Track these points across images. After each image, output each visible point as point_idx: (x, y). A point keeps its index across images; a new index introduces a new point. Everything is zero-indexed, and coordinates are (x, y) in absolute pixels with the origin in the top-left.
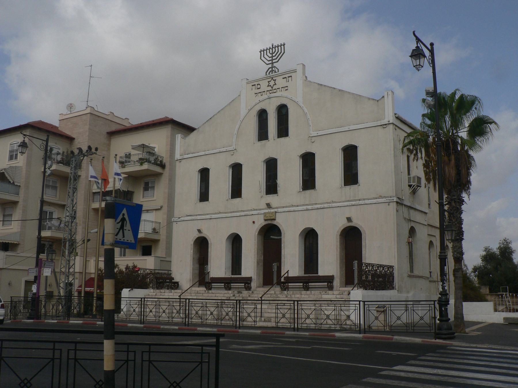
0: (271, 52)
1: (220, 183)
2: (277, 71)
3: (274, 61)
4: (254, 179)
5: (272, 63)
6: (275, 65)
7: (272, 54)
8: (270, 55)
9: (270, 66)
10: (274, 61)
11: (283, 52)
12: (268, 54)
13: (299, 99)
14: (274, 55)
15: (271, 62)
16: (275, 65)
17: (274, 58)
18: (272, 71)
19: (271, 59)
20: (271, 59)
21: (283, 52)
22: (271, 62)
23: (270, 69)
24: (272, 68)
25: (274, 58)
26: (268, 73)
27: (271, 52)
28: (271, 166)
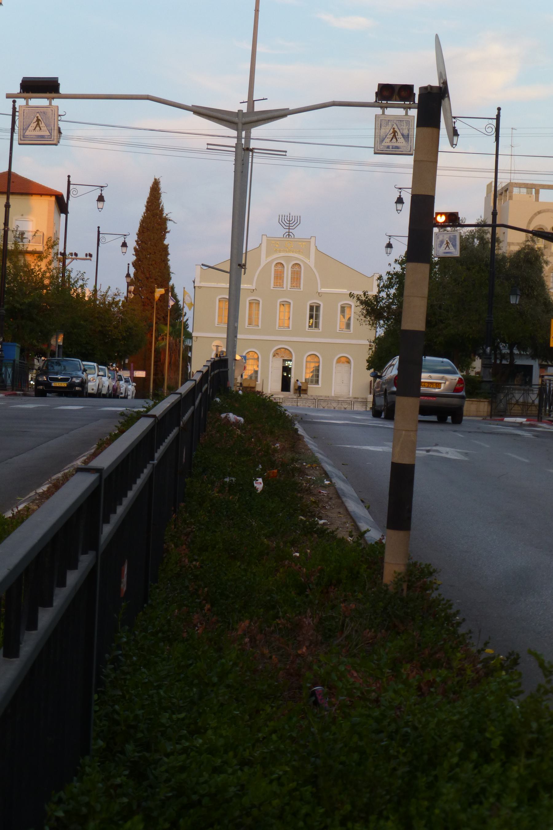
2: (293, 236)
3: (290, 228)
6: (291, 231)
9: (287, 230)
14: (291, 222)
16: (291, 231)
24: (289, 232)
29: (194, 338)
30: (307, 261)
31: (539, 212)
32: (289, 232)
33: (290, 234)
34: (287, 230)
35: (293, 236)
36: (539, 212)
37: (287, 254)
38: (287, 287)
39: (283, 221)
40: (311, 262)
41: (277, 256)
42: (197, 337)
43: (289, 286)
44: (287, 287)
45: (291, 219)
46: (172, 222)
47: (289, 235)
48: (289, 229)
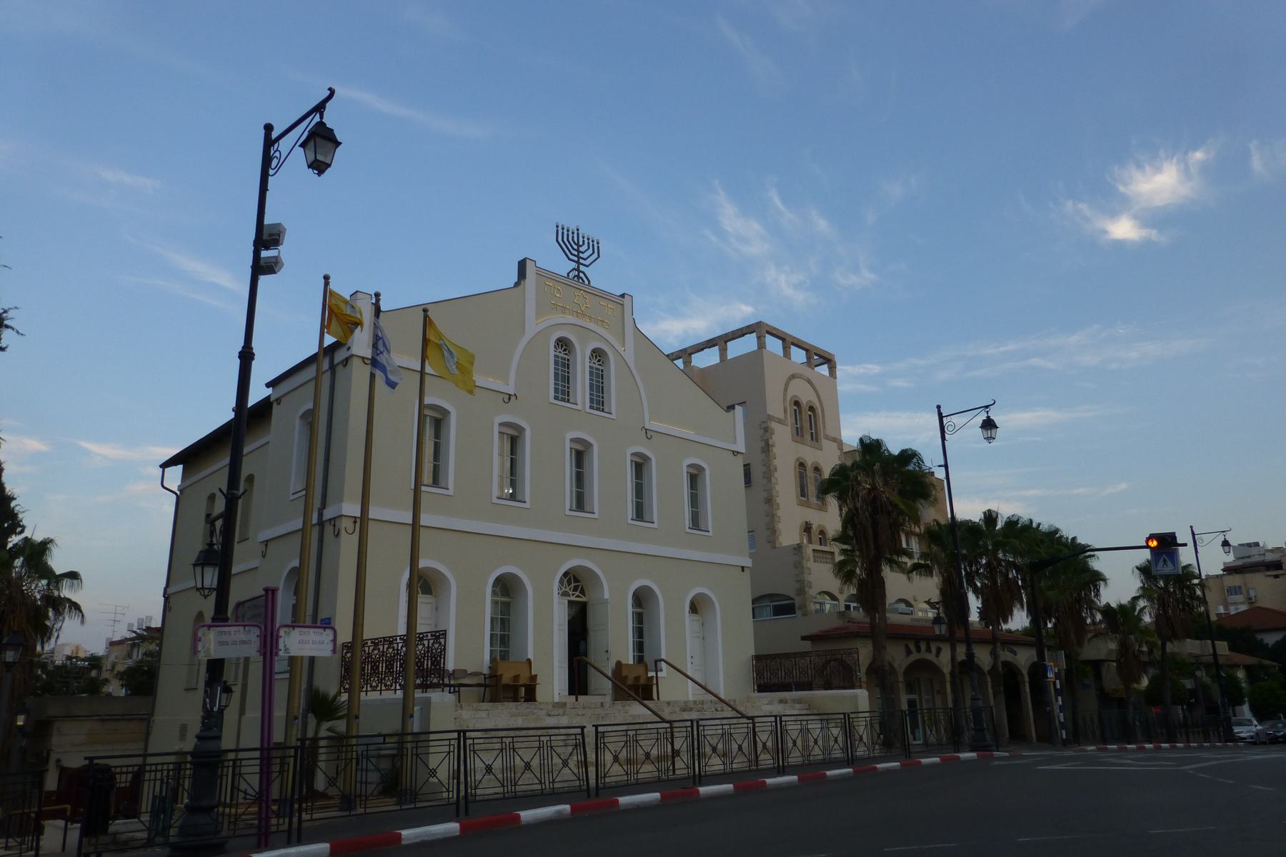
6: (582, 268)
7: (578, 244)
9: (574, 265)
13: (629, 355)
14: (582, 249)
18: (578, 276)
26: (571, 275)
30: (621, 349)
31: (793, 377)
32: (579, 272)
34: (574, 265)
36: (793, 377)
37: (579, 322)
38: (584, 404)
40: (629, 355)
41: (561, 322)
43: (588, 404)
44: (584, 404)
46: (14, 333)
47: (578, 276)
48: (578, 262)
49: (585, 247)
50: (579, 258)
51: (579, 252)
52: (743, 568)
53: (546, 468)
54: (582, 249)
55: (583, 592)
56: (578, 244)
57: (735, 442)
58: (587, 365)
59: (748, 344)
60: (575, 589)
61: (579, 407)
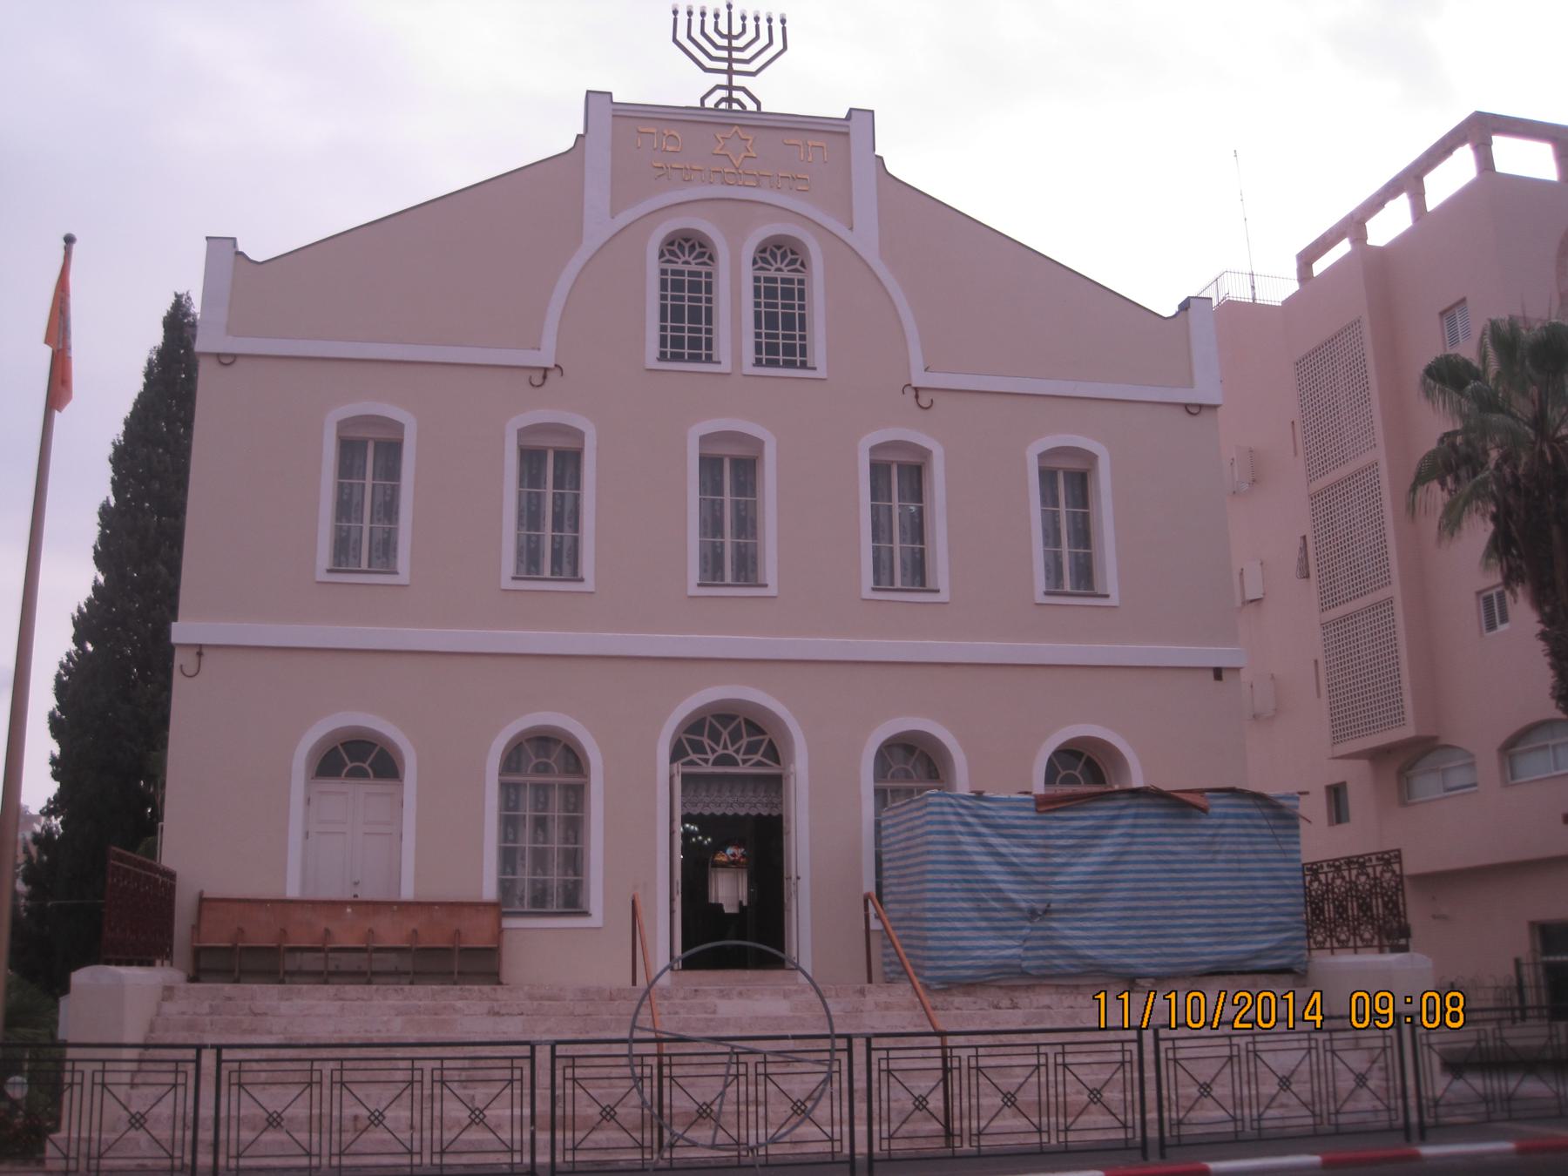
0: (724, 29)
1: (460, 498)
2: (751, 106)
3: (736, 67)
4: (639, 508)
5: (730, 72)
6: (738, 81)
7: (730, 37)
8: (725, 42)
9: (723, 79)
10: (736, 67)
11: (778, 45)
12: (709, 30)
13: (866, 237)
14: (735, 43)
15: (724, 66)
17: (736, 55)
18: (730, 100)
19: (725, 54)
20: (725, 54)
21: (778, 45)
22: (724, 66)
23: (724, 93)
25: (736, 55)
26: (710, 103)
27: (724, 29)
28: (731, 471)
29: (180, 659)
32: (730, 87)
33: (736, 94)
34: (723, 79)
35: (751, 106)
39: (696, 33)
40: (866, 237)
42: (200, 650)
43: (749, 354)
45: (736, 30)
47: (730, 100)
48: (730, 72)
49: (750, 34)
50: (730, 60)
51: (730, 49)
52: (1218, 673)
53: (639, 508)
54: (735, 43)
55: (773, 754)
56: (730, 37)
57: (1191, 385)
58: (748, 273)
59: (1459, 170)
60: (752, 748)
61: (725, 367)
